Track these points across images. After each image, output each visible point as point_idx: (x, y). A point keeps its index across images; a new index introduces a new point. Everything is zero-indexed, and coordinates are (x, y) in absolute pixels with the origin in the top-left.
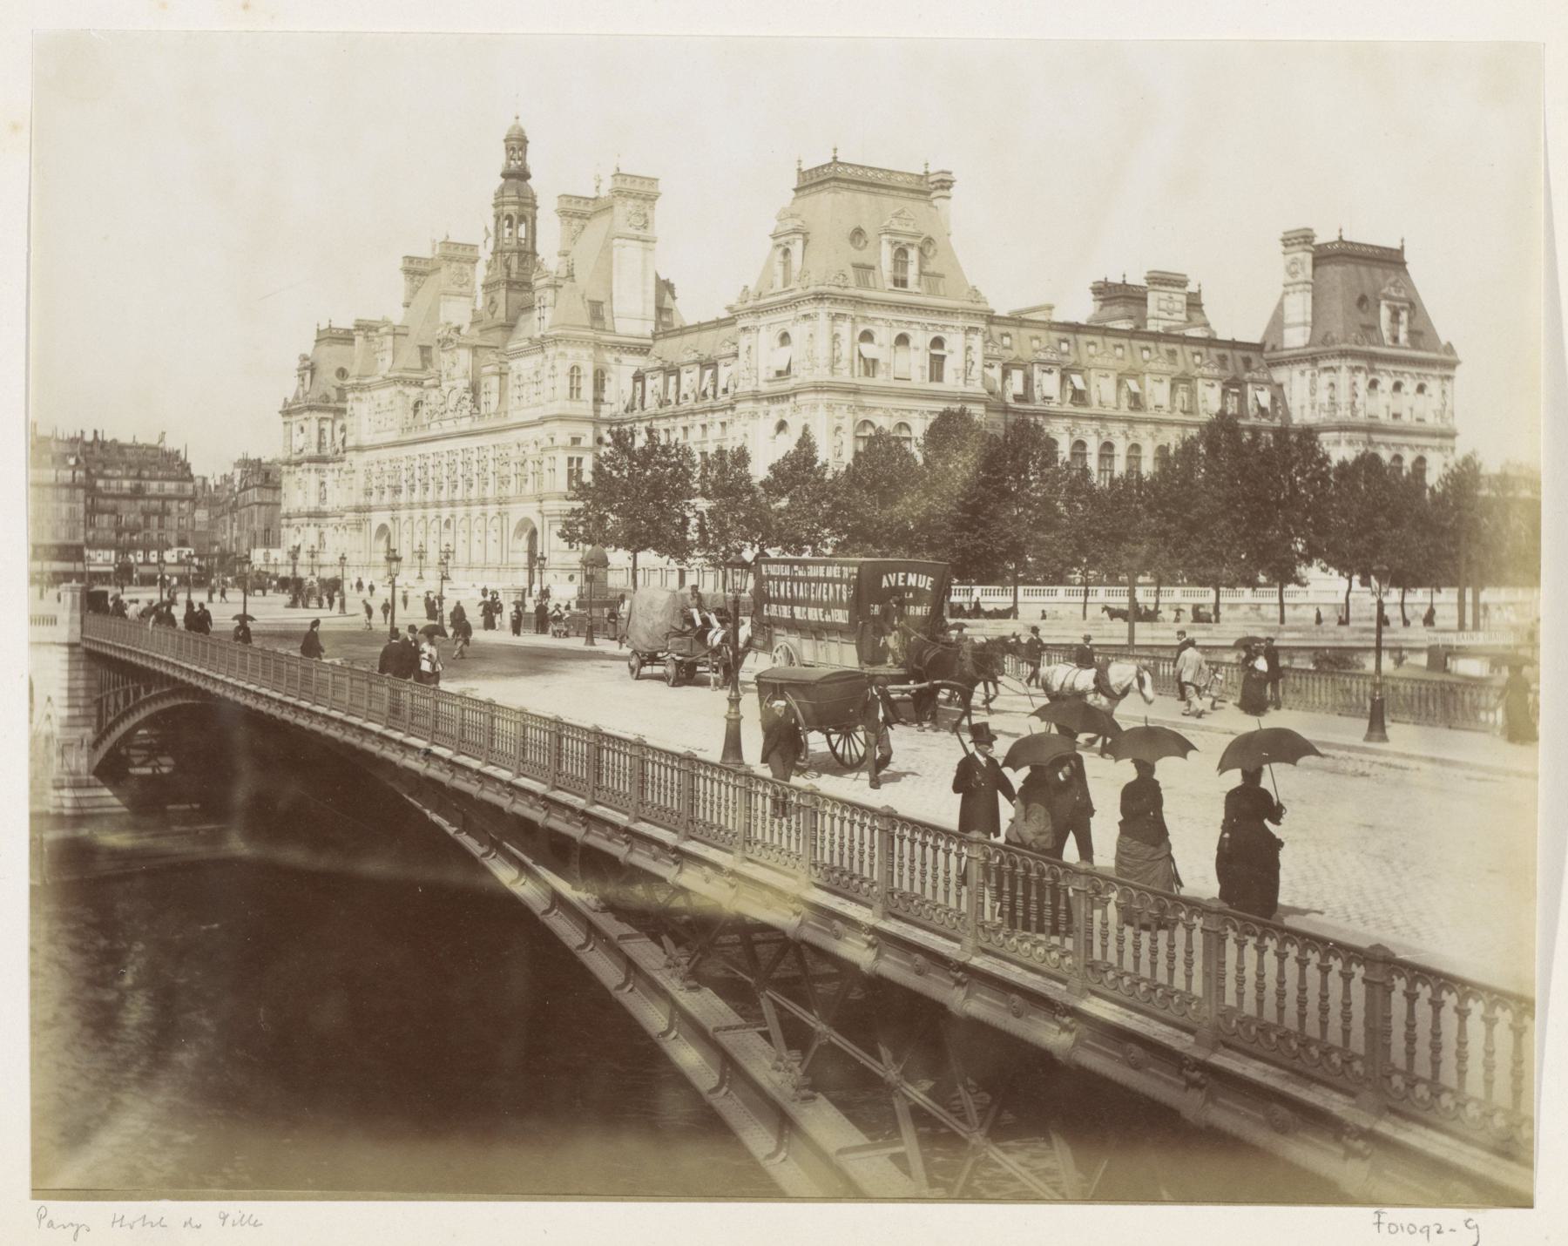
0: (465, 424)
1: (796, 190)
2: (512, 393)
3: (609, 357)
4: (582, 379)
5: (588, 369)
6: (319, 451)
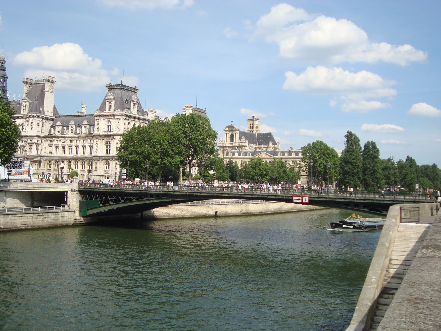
3: (44, 121)
4: (39, 126)
5: (41, 124)
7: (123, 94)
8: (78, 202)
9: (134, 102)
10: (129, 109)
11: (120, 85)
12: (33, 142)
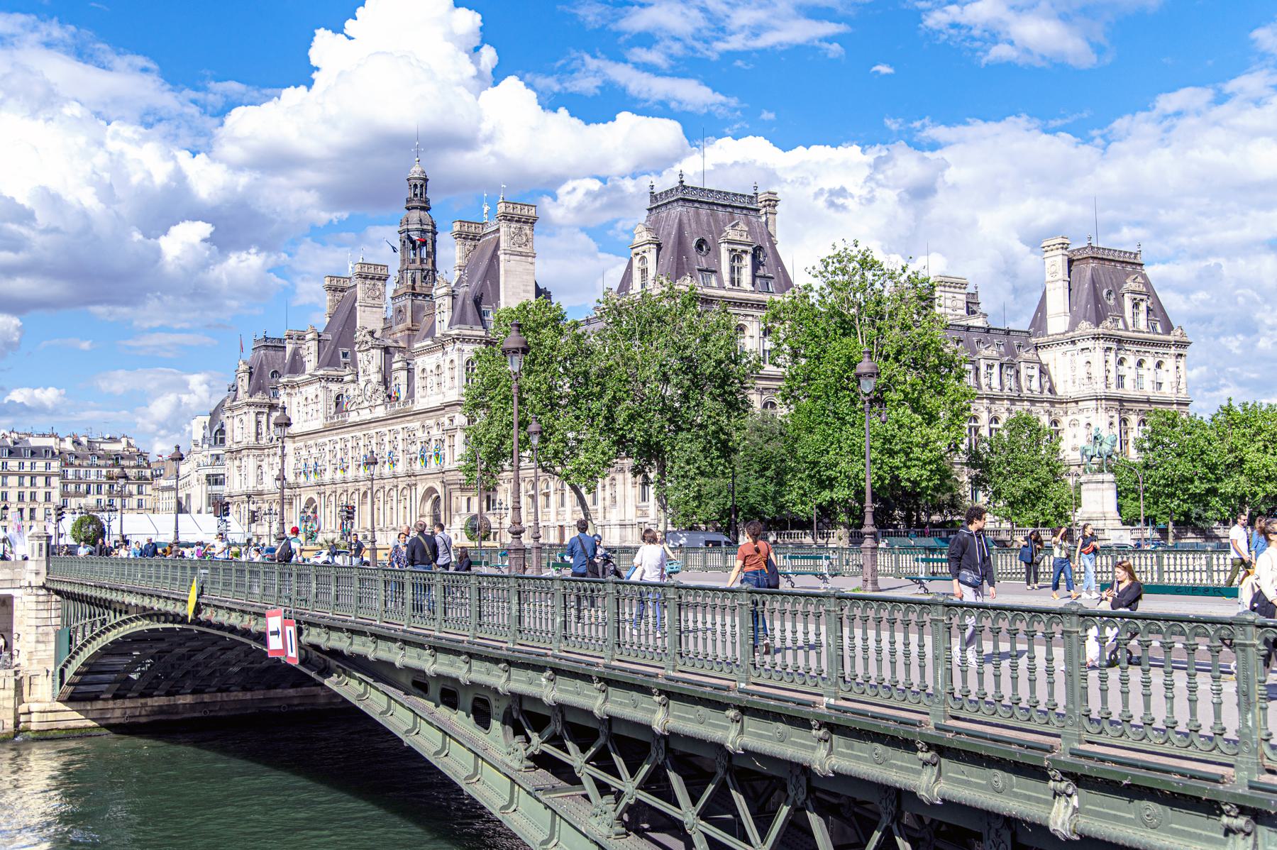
0: (380, 412)
1: (650, 210)
2: (418, 382)
6: (257, 439)
7: (685, 220)
8: (52, 638)
9: (735, 247)
10: (714, 272)
11: (677, 188)
12: (456, 422)
